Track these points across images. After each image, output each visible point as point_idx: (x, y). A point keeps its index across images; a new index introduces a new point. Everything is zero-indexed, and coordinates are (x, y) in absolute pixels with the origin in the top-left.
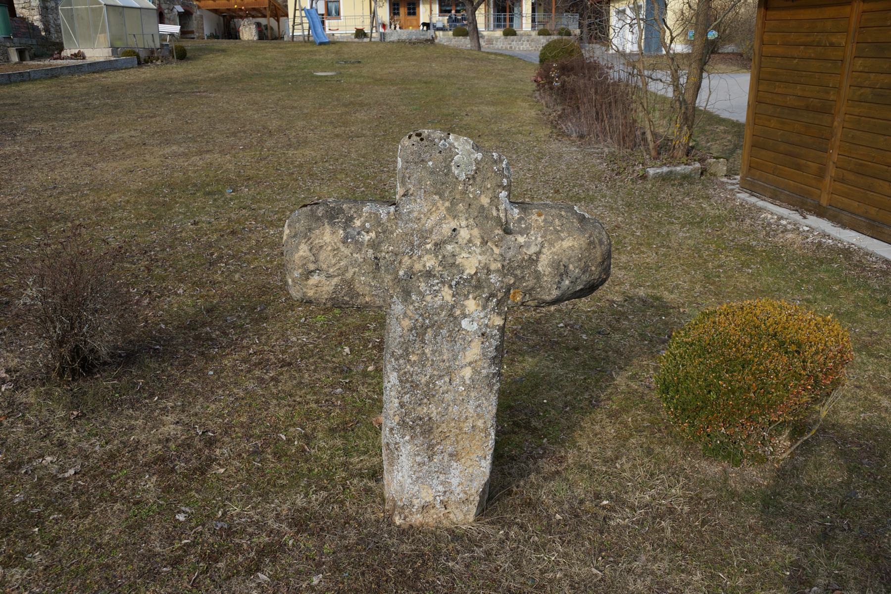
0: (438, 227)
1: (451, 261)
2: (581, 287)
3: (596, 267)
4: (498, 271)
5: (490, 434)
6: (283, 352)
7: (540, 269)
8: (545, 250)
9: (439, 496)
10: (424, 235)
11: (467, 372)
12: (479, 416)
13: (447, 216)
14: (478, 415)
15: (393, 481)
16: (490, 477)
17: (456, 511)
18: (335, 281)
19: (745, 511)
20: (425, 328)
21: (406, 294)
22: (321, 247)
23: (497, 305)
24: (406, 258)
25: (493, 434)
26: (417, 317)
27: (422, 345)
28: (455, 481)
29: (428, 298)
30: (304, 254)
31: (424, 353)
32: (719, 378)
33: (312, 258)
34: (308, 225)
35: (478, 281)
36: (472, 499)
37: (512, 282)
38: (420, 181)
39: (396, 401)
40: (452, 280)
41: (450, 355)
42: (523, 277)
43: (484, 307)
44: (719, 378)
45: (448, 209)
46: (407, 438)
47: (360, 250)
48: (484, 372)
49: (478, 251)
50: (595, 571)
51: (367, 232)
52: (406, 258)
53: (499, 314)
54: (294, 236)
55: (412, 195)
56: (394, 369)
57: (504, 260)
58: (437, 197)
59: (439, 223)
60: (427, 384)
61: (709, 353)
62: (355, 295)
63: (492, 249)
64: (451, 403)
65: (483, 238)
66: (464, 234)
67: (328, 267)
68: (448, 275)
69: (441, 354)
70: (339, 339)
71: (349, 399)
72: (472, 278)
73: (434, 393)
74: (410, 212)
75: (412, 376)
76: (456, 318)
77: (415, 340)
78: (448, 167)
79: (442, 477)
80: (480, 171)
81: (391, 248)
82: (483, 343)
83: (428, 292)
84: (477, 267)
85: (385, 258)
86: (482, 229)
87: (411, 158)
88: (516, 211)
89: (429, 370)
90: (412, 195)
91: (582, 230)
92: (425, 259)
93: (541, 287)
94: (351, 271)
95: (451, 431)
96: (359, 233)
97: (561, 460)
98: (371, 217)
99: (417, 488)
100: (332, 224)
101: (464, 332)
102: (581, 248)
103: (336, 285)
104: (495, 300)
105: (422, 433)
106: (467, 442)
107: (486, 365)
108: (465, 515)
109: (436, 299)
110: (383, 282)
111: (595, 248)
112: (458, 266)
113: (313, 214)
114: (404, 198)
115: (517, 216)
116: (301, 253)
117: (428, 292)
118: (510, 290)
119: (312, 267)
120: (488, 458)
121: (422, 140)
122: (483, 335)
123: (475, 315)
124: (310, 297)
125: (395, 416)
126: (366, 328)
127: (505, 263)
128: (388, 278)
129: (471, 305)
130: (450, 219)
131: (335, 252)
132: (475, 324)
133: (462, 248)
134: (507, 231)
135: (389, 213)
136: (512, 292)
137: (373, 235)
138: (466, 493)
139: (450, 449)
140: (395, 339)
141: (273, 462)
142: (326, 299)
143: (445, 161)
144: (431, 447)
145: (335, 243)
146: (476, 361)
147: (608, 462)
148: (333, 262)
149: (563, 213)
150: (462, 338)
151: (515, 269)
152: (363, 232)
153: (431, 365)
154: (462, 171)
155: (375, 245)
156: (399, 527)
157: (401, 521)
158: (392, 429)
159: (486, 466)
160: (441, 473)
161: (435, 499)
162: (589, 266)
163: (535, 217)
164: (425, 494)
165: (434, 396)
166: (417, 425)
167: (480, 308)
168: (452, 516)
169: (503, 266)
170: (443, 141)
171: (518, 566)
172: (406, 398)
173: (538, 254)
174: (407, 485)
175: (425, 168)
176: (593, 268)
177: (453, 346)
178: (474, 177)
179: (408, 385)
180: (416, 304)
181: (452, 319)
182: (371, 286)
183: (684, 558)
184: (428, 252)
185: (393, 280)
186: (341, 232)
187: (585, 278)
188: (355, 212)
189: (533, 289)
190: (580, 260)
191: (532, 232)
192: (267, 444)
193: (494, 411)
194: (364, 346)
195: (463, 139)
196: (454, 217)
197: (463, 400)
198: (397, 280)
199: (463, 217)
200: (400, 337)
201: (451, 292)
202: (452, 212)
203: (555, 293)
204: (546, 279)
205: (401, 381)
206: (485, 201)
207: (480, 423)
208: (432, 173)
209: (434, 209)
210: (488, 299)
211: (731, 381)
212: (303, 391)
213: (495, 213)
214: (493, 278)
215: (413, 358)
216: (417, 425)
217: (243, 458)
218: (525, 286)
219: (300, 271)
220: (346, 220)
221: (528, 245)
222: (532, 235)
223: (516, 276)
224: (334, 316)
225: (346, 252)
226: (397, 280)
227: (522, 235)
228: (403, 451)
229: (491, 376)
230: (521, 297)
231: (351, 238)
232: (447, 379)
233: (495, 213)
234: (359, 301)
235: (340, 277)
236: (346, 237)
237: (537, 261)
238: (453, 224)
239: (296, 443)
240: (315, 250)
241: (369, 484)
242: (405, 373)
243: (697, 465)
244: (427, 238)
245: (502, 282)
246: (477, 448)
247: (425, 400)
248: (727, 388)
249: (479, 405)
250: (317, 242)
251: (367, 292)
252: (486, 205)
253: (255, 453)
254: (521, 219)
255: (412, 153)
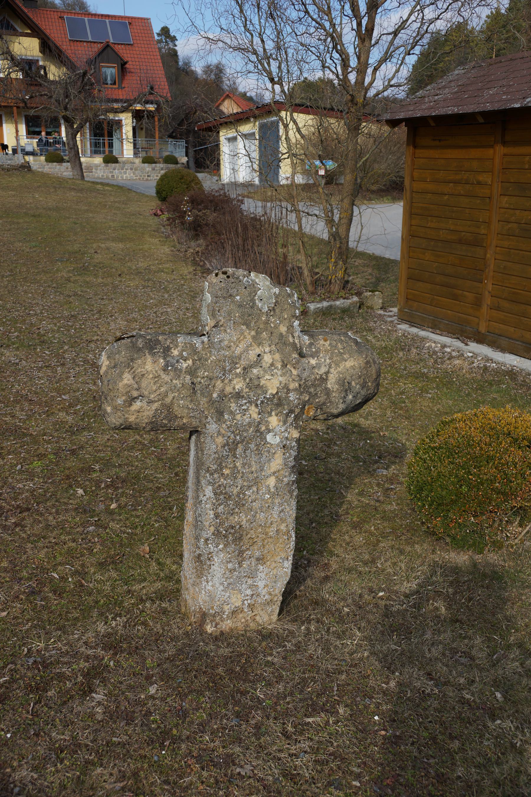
0: (245, 354)
1: (256, 383)
2: (360, 400)
3: (372, 383)
4: (295, 390)
5: (291, 536)
6: (15, 499)
7: (329, 386)
8: (332, 370)
9: (247, 600)
10: (234, 361)
11: (272, 482)
12: (283, 520)
13: (253, 343)
14: (281, 519)
15: (200, 592)
16: (292, 576)
17: (261, 613)
18: (156, 405)
19: (498, 588)
20: (236, 444)
21: (220, 413)
22: (143, 375)
23: (295, 419)
24: (219, 382)
25: (294, 536)
26: (229, 434)
27: (234, 459)
28: (261, 584)
29: (238, 417)
30: (128, 382)
31: (235, 467)
32: (469, 473)
33: (136, 386)
34: (130, 356)
35: (279, 399)
36: (275, 599)
37: (307, 398)
38: (229, 314)
39: (212, 512)
40: (257, 400)
41: (258, 466)
42: (316, 394)
43: (285, 422)
44: (469, 473)
45: (254, 338)
46: (221, 546)
47: (179, 376)
48: (286, 480)
49: (279, 373)
50: (394, 647)
51: (185, 360)
52: (219, 382)
53: (296, 428)
54: (115, 367)
55: (221, 326)
56: (210, 483)
57: (301, 380)
58: (244, 327)
59: (246, 350)
60: (239, 494)
61: (456, 454)
62: (171, 416)
63: (290, 371)
64: (258, 510)
65: (283, 362)
66: (267, 359)
67: (150, 393)
68: (254, 396)
69: (250, 466)
70: (67, 482)
71: (104, 535)
72: (274, 397)
73: (244, 502)
74: (220, 341)
75: (225, 488)
76: (262, 433)
77: (228, 455)
78: (253, 300)
79: (250, 581)
80: (278, 304)
81: (206, 374)
82: (284, 454)
83: (238, 411)
84: (278, 388)
85: (200, 383)
86: (282, 353)
87: (220, 293)
88: (306, 337)
89: (240, 482)
90: (221, 326)
91: (360, 352)
92: (235, 382)
93: (330, 402)
94: (171, 396)
95: (258, 537)
96: (178, 361)
97: (327, 566)
98: (187, 347)
99: (228, 594)
100: (153, 355)
101: (268, 445)
102: (360, 367)
103: (156, 410)
104: (293, 416)
105: (234, 541)
106: (272, 546)
107: (287, 474)
108: (270, 616)
109: (245, 417)
110: (199, 404)
111: (370, 366)
112: (262, 387)
113: (134, 345)
114: (214, 329)
115: (308, 342)
116: (125, 381)
117: (238, 411)
118: (305, 406)
119: (135, 394)
120: (290, 558)
121: (228, 277)
122: (284, 447)
123: (277, 429)
124: (130, 422)
125: (210, 526)
126: (91, 470)
127: (302, 383)
128: (204, 401)
129: (274, 421)
130: (256, 346)
131: (156, 379)
132: (278, 437)
133: (265, 371)
134: (302, 355)
135: (203, 342)
136: (306, 407)
137: (190, 362)
138: (270, 594)
139: (257, 554)
140: (210, 455)
141: (55, 600)
142: (147, 424)
143: (250, 296)
144: (241, 553)
145: (156, 372)
146: (279, 471)
147: (367, 563)
148: (154, 388)
149: (342, 338)
150: (267, 451)
151: (310, 387)
152: (181, 360)
153: (242, 477)
154: (264, 304)
155: (192, 372)
156: (211, 634)
157: (213, 629)
158: (207, 540)
159: (288, 565)
160: (249, 577)
161: (243, 604)
162: (366, 383)
163: (322, 342)
164: (234, 600)
165: (243, 505)
166: (230, 533)
167: (281, 423)
168: (258, 618)
169: (300, 385)
170: (246, 279)
171: (328, 652)
172: (221, 509)
173: (327, 373)
174: (219, 593)
175: (233, 302)
176: (370, 384)
177: (260, 458)
178: (274, 309)
179: (222, 497)
180: (228, 423)
181: (258, 434)
182: (188, 408)
183: (461, 628)
184: (237, 375)
185: (208, 402)
186: (162, 361)
187: (363, 392)
188: (171, 343)
189: (324, 404)
190: (360, 377)
191: (321, 355)
192: (41, 583)
193: (294, 515)
194: (95, 486)
195: (261, 276)
196: (259, 344)
197: (269, 506)
198: (211, 402)
199: (267, 344)
200: (215, 453)
201: (257, 410)
202: (257, 340)
203: (342, 407)
204: (334, 394)
205: (215, 494)
206: (283, 329)
207: (283, 527)
208: (240, 306)
209: (242, 338)
210: (287, 415)
211: (479, 475)
212: (55, 533)
213: (291, 340)
214: (292, 396)
215: (226, 471)
216: (230, 533)
217: (22, 600)
218: (319, 402)
219: (124, 398)
220: (164, 350)
221: (318, 366)
222: (321, 358)
223: (310, 394)
224: (51, 462)
225: (166, 379)
226: (211, 402)
227: (313, 358)
228: (216, 560)
229: (291, 483)
230: (314, 411)
231: (171, 366)
232: (255, 489)
233: (291, 340)
234: (176, 423)
235: (160, 402)
236: (167, 365)
237: (326, 380)
238: (258, 351)
239: (70, 579)
240: (138, 378)
241: (163, 605)
242: (220, 486)
243: (447, 557)
244: (237, 363)
245: (299, 399)
246: (280, 551)
247: (237, 510)
248: (476, 481)
249: (283, 511)
250: (139, 370)
251: (185, 415)
252: (284, 333)
253: (33, 593)
254: (311, 344)
255: (220, 289)
